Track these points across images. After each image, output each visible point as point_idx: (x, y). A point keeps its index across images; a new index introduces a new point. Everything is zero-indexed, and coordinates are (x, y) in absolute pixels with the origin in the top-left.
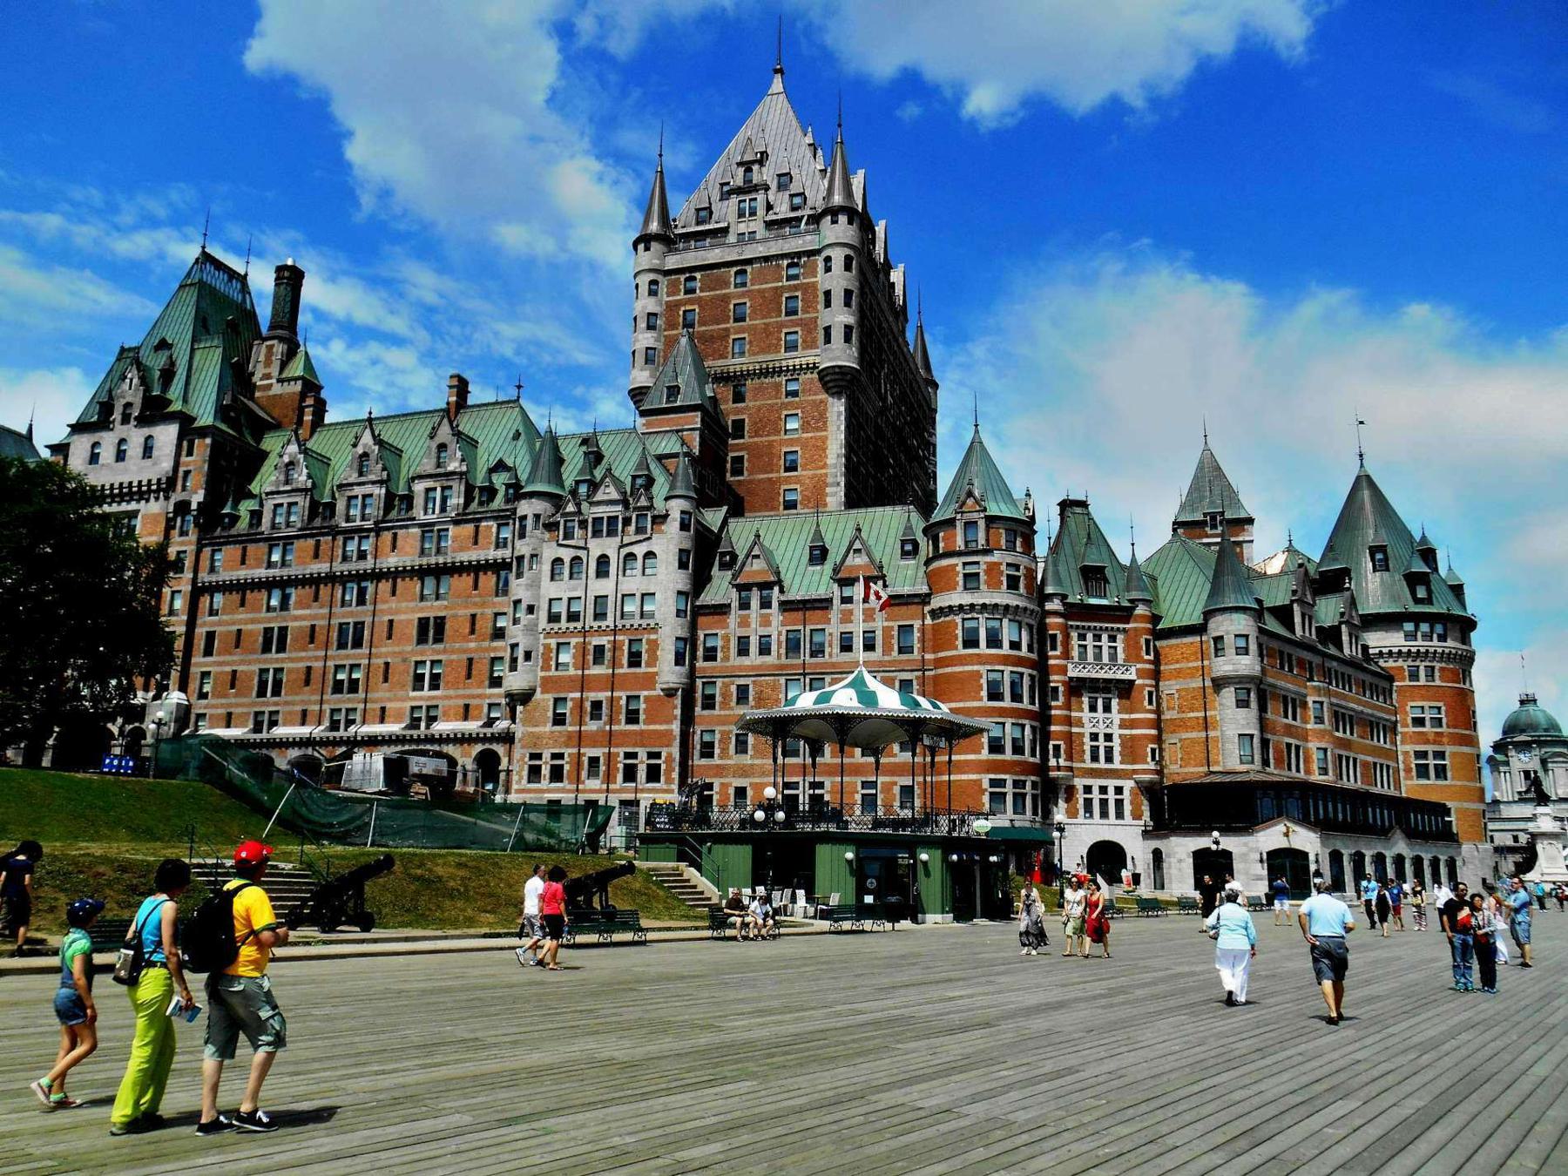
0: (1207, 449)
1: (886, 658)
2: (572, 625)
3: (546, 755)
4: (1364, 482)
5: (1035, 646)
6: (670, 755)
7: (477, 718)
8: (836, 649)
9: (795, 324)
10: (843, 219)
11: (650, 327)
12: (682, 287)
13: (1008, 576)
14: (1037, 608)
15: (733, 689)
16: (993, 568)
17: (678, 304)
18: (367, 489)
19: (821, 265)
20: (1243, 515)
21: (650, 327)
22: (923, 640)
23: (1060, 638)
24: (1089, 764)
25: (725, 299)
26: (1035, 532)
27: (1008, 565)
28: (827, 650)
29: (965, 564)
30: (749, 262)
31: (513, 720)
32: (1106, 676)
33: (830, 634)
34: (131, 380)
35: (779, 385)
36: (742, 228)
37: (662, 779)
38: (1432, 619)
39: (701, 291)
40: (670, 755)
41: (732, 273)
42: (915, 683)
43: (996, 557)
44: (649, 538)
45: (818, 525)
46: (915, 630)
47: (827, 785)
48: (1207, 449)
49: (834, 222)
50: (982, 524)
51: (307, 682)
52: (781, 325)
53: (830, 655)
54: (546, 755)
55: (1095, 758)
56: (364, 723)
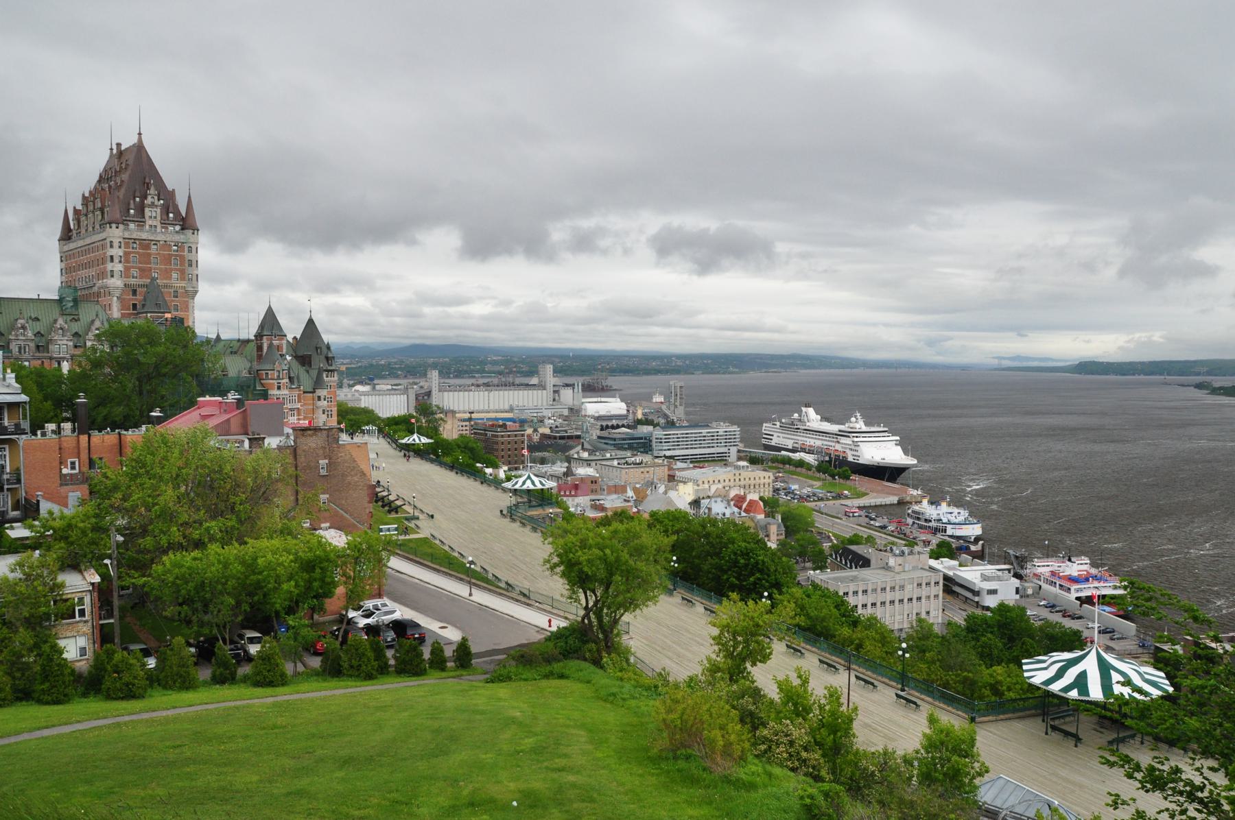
9: (176, 270)
11: (120, 262)
18: (65, 342)
19: (186, 249)
21: (120, 262)
25: (149, 255)
38: (331, 371)
49: (193, 233)
52: (171, 270)
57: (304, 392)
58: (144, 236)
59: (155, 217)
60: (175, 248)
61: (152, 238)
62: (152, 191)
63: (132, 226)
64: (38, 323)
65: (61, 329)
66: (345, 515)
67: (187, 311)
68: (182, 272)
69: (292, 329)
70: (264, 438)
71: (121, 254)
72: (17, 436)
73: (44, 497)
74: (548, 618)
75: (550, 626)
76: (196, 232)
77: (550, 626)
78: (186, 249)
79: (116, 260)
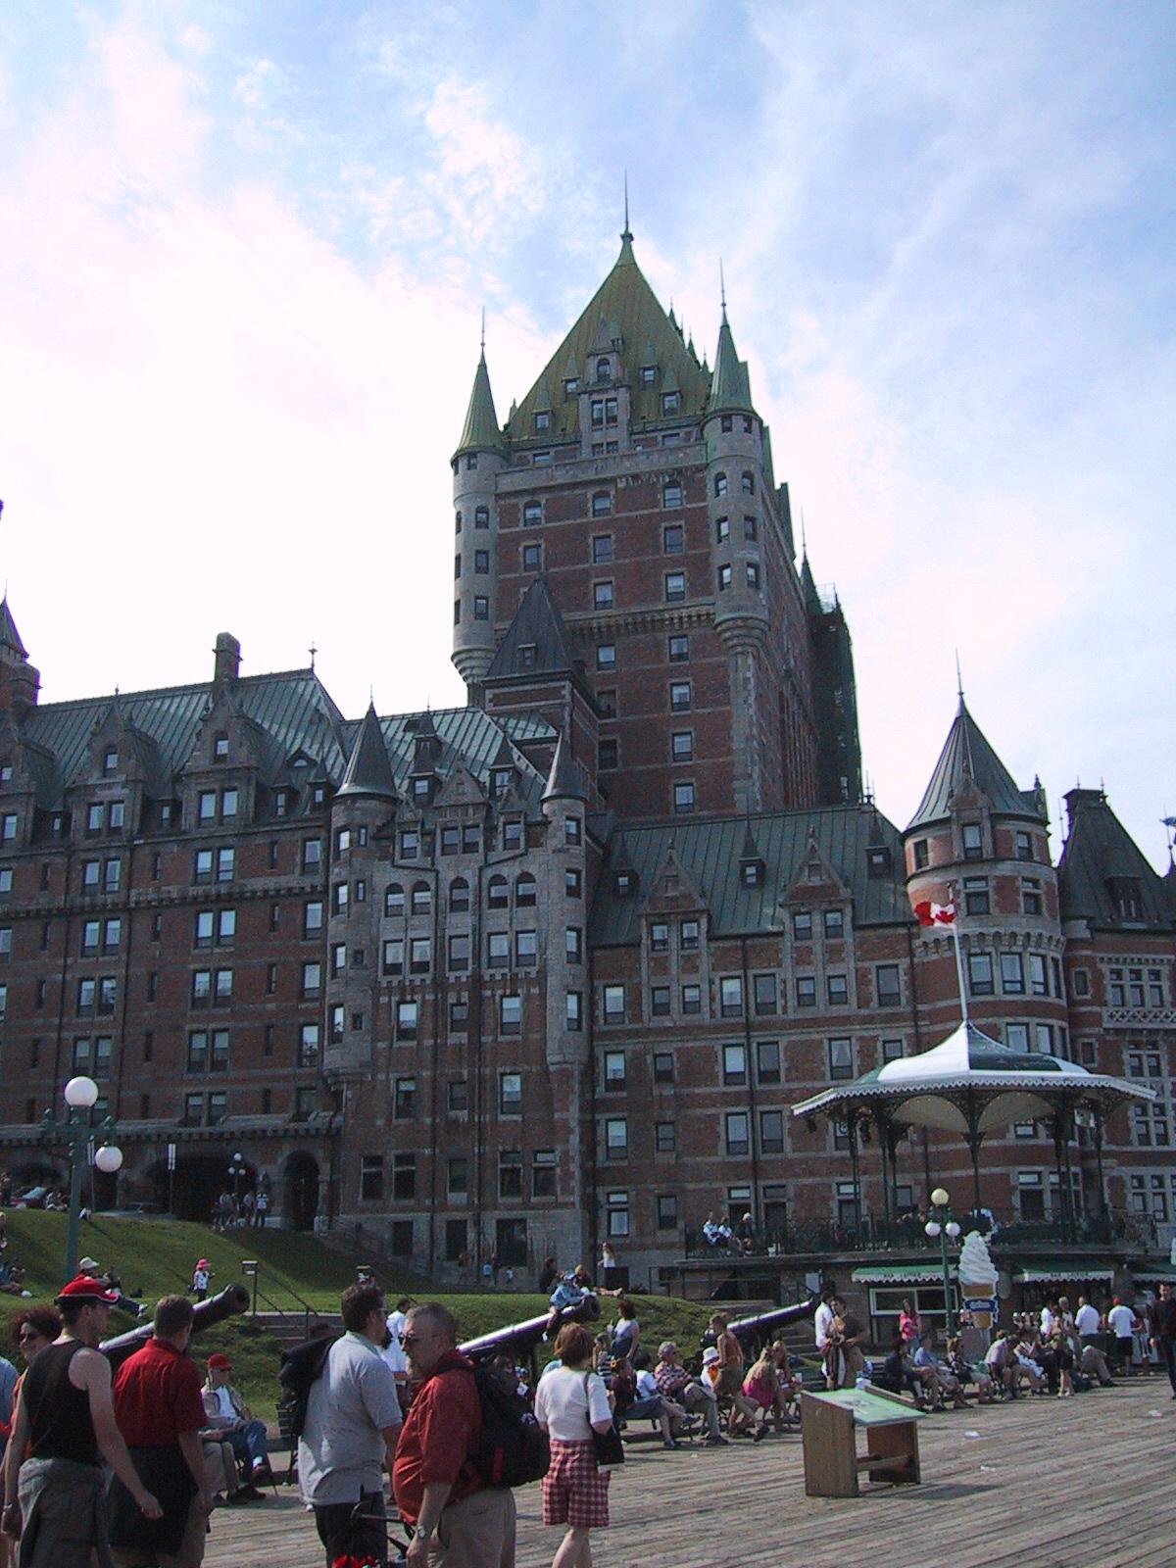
1: (864, 1012)
2: (418, 978)
3: (390, 1158)
5: (1063, 988)
6: (566, 1153)
7: (283, 1109)
8: (792, 1002)
9: (679, 562)
10: (738, 424)
12: (520, 516)
13: (1026, 895)
14: (1063, 939)
15: (649, 1059)
16: (1005, 885)
17: (516, 539)
19: (710, 485)
22: (912, 985)
23: (1089, 976)
24: (1137, 1148)
25: (582, 531)
26: (1049, 835)
27: (1025, 879)
28: (780, 1003)
29: (967, 880)
30: (613, 480)
31: (338, 1109)
32: (1151, 1026)
33: (784, 982)
35: (659, 646)
36: (598, 437)
37: (559, 1190)
40: (566, 1153)
41: (590, 496)
42: (905, 1043)
43: (1005, 869)
44: (521, 855)
45: (749, 829)
46: (901, 973)
47: (791, 1190)
49: (729, 429)
50: (987, 825)
51: (35, 1062)
53: (785, 1008)
54: (390, 1158)
55: (1145, 1139)
56: (118, 1117)
61: (591, 475)
78: (710, 485)
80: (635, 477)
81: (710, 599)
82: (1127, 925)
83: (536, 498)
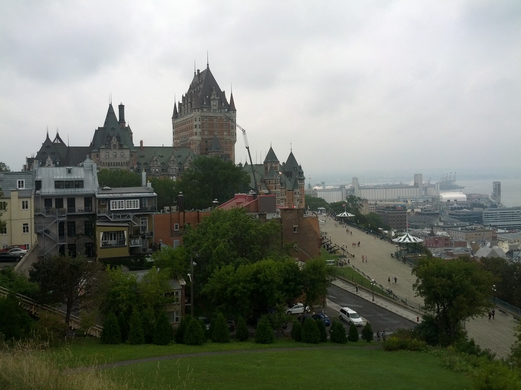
0: (271, 147)
4: (291, 155)
9: (226, 131)
11: (200, 128)
17: (204, 123)
18: (175, 167)
20: (278, 161)
21: (200, 128)
30: (218, 117)
34: (114, 139)
39: (209, 121)
48: (271, 147)
50: (277, 180)
52: (224, 131)
57: (288, 190)
58: (211, 114)
59: (216, 105)
60: (225, 120)
61: (214, 116)
62: (214, 92)
63: (205, 110)
64: (163, 158)
65: (173, 161)
66: (306, 254)
67: (232, 151)
68: (229, 132)
69: (282, 158)
70: (266, 214)
71: (200, 124)
72: (151, 213)
73: (162, 242)
74: (417, 316)
75: (418, 321)
76: (235, 111)
77: (418, 321)
79: (198, 127)
80: (220, 117)
81: (230, 137)
82: (282, 188)
83: (207, 117)
